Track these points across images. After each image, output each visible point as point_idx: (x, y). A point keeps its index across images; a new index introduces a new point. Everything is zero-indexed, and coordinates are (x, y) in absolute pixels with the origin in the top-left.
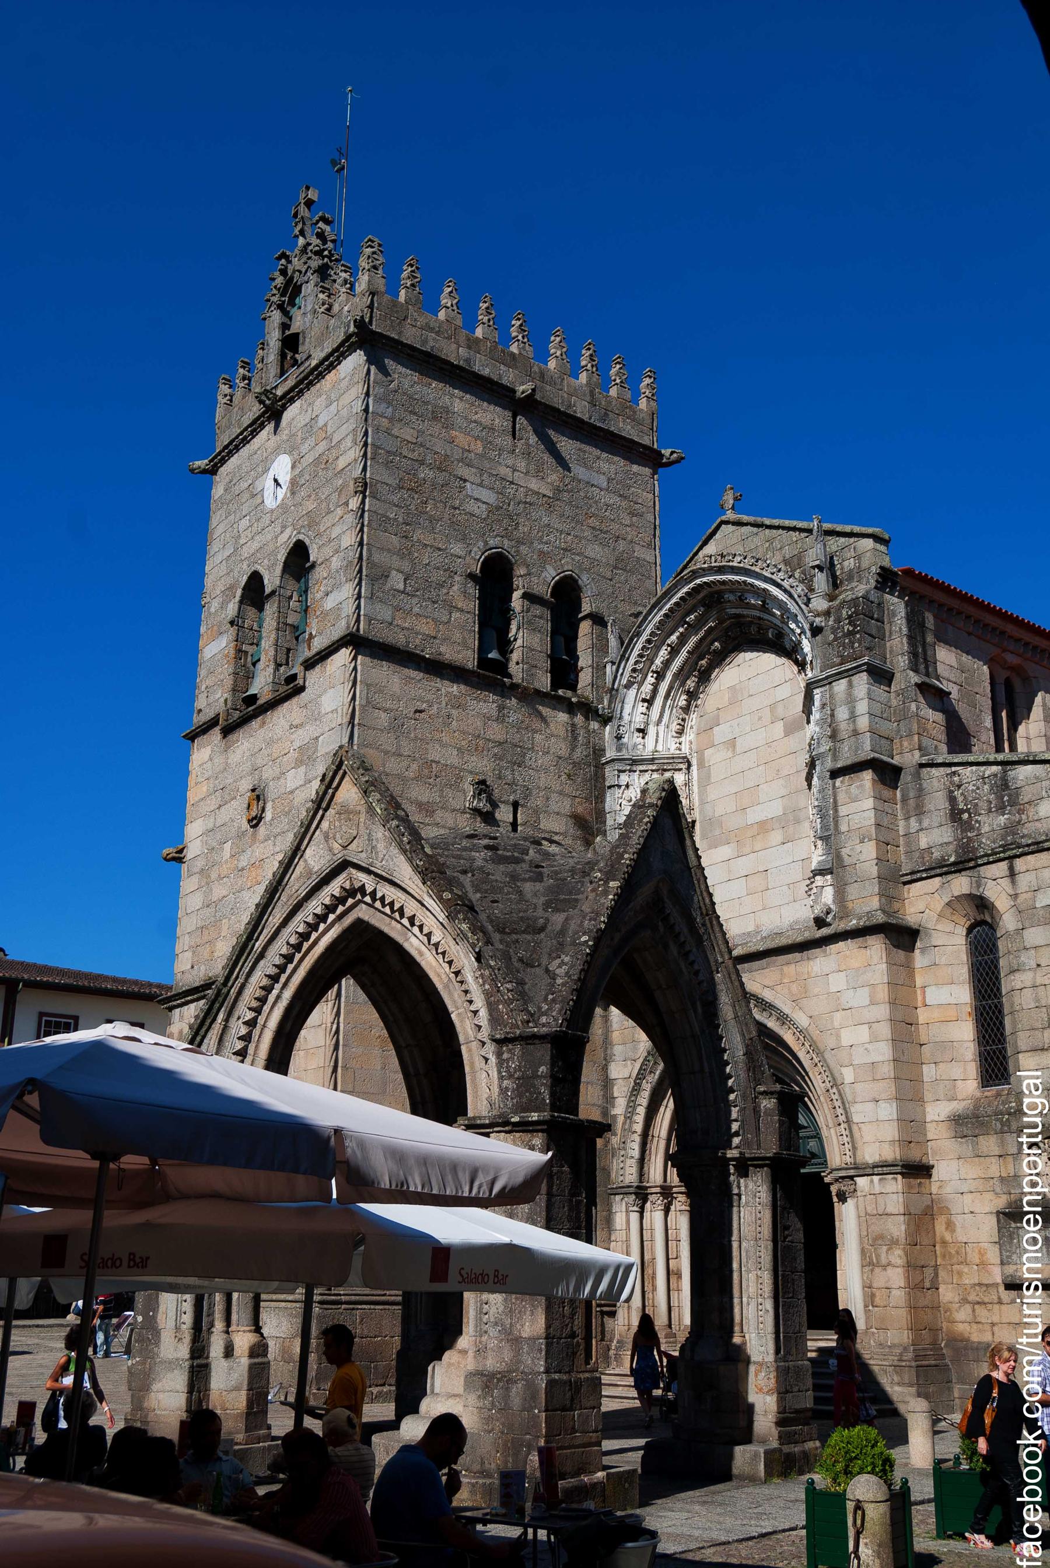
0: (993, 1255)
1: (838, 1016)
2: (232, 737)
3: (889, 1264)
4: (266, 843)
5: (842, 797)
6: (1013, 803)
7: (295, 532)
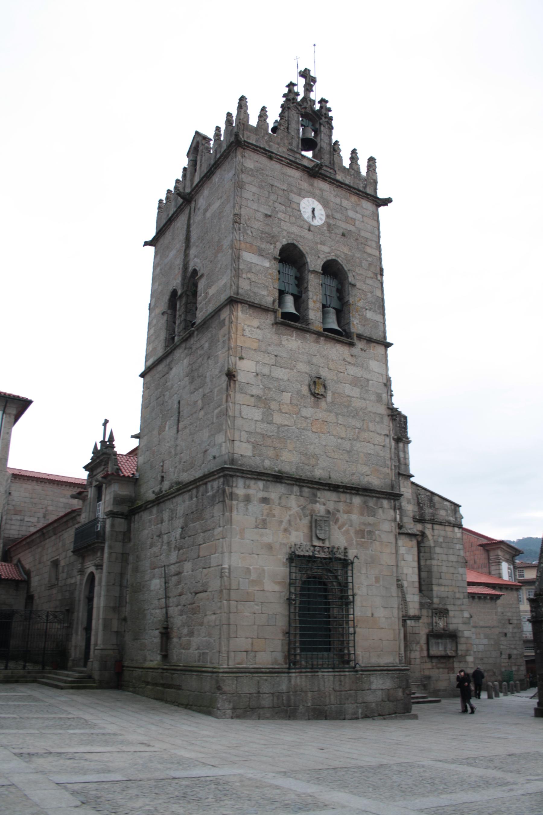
0: (425, 647)
1: (403, 562)
2: (282, 329)
3: (416, 650)
4: (328, 413)
5: (401, 485)
6: (434, 506)
7: (333, 254)
